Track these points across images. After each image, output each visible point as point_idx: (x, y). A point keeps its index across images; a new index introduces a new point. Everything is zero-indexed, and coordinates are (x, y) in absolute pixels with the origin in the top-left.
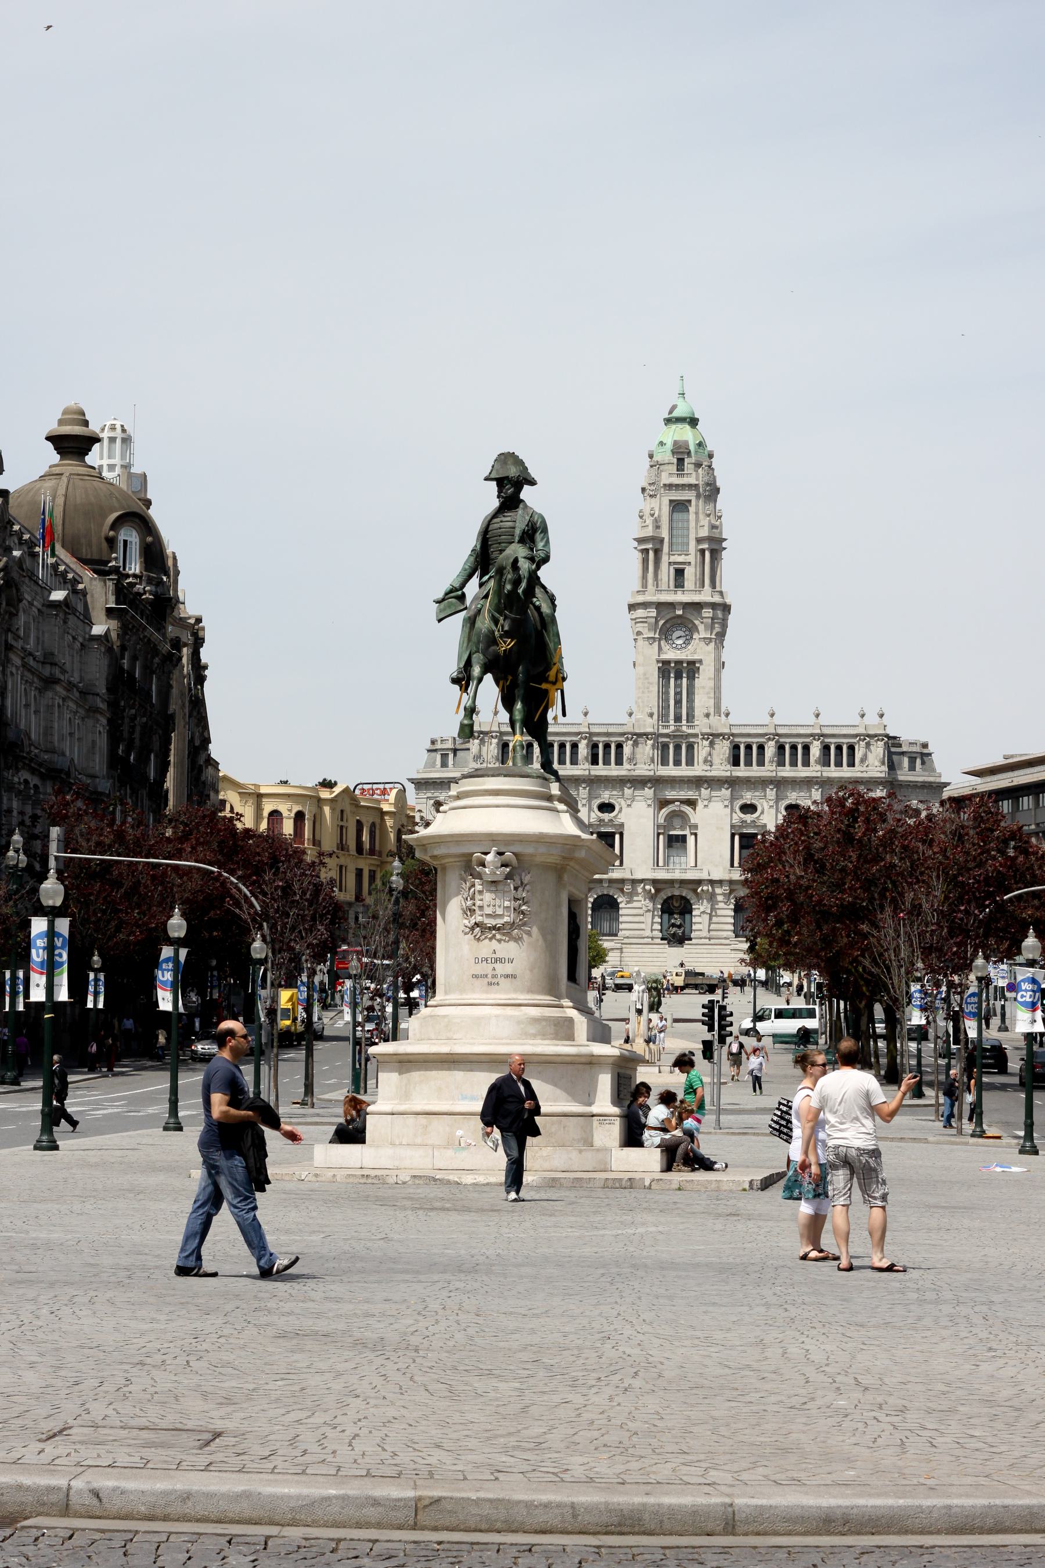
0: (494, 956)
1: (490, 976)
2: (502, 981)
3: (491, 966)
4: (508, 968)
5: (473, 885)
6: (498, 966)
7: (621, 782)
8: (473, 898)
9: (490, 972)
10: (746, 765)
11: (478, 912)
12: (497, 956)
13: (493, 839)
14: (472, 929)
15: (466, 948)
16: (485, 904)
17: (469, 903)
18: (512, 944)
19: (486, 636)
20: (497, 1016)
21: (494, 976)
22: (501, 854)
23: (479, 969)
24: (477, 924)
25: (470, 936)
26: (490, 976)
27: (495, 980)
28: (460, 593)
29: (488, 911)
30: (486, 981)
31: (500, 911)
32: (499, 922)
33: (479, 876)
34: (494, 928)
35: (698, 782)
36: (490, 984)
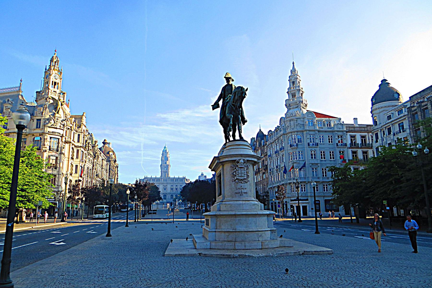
2: (244, 194)
4: (245, 191)
5: (235, 169)
6: (242, 190)
7: (160, 183)
8: (235, 172)
9: (240, 191)
11: (237, 175)
13: (241, 155)
14: (235, 180)
15: (233, 186)
18: (246, 184)
20: (245, 204)
21: (242, 193)
22: (243, 160)
23: (237, 191)
24: (237, 179)
29: (240, 175)
31: (243, 175)
32: (242, 178)
33: (237, 166)
34: (241, 180)
35: (167, 183)
36: (241, 195)
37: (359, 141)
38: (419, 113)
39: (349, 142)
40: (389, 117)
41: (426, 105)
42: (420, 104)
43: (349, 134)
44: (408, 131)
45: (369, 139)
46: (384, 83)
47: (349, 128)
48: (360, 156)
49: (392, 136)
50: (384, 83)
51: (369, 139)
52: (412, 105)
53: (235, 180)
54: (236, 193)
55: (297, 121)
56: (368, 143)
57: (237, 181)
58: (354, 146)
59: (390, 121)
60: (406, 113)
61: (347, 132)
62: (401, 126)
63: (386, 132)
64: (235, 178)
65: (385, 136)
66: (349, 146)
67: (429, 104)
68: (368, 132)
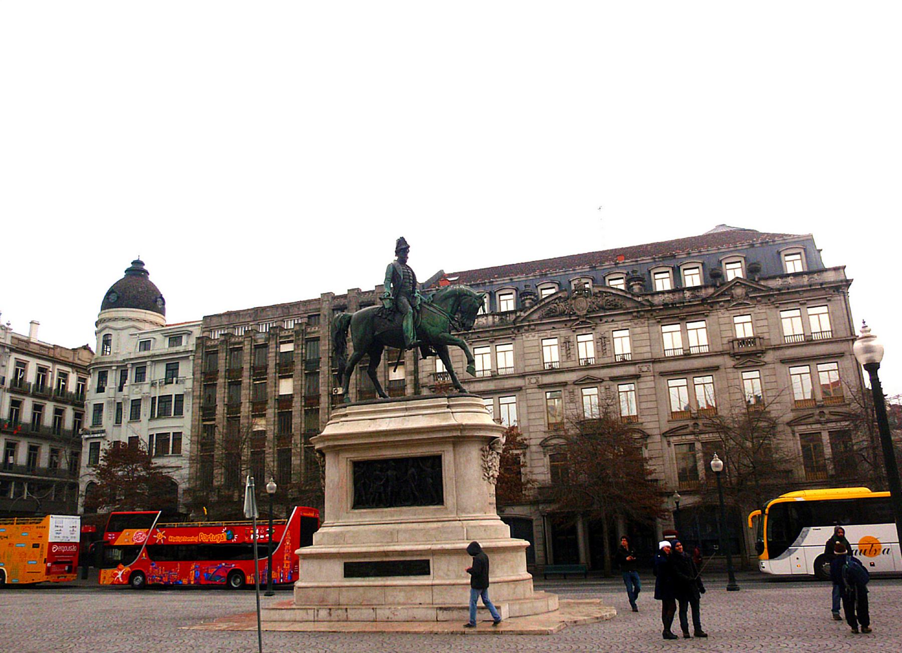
37: (31, 377)
38: (222, 355)
39: (10, 376)
40: (145, 345)
41: (240, 343)
42: (227, 338)
43: (15, 355)
44: (189, 384)
45: (52, 378)
46: (137, 270)
47: (16, 342)
48: (26, 415)
49: (146, 388)
50: (137, 270)
51: (52, 378)
52: (206, 334)
56: (49, 386)
58: (17, 388)
59: (146, 353)
60: (192, 348)
61: (12, 350)
62: (172, 371)
63: (131, 375)
65: (128, 383)
66: (7, 384)
67: (246, 343)
68: (55, 361)
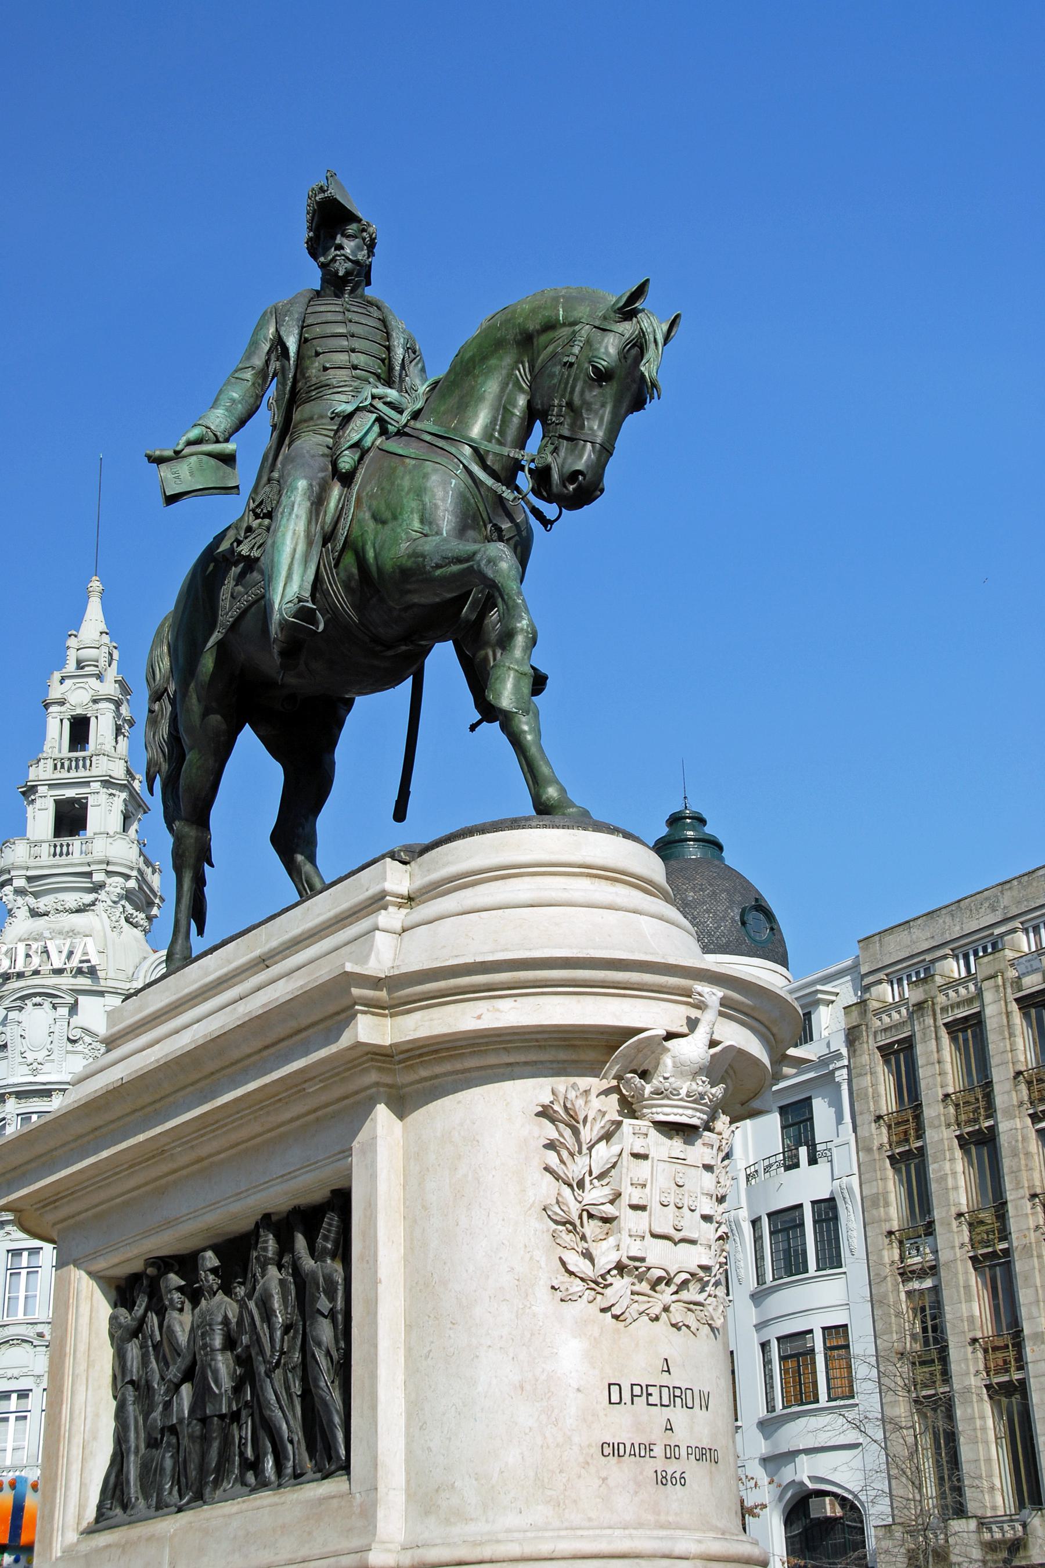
0: (665, 1379)
1: (658, 1451)
3: (660, 1415)
6: (678, 1415)
10: (720, 1011)
12: (676, 1379)
14: (599, 1284)
16: (650, 1196)
17: (596, 1194)
19: (462, 500)
21: (671, 1452)
24: (621, 1268)
25: (583, 1308)
26: (658, 1451)
27: (672, 1467)
28: (230, 447)
30: (650, 1466)
36: (663, 1480)
53: (599, 1284)
54: (614, 1450)
55: (73, 1009)
57: (621, 1285)
64: (607, 1255)
